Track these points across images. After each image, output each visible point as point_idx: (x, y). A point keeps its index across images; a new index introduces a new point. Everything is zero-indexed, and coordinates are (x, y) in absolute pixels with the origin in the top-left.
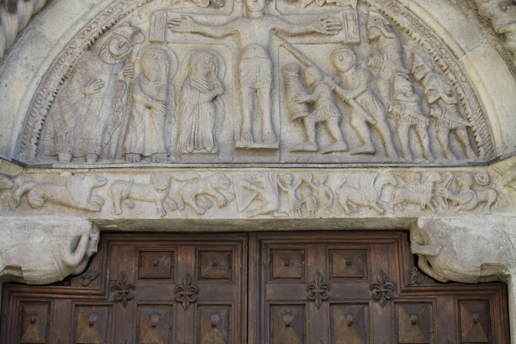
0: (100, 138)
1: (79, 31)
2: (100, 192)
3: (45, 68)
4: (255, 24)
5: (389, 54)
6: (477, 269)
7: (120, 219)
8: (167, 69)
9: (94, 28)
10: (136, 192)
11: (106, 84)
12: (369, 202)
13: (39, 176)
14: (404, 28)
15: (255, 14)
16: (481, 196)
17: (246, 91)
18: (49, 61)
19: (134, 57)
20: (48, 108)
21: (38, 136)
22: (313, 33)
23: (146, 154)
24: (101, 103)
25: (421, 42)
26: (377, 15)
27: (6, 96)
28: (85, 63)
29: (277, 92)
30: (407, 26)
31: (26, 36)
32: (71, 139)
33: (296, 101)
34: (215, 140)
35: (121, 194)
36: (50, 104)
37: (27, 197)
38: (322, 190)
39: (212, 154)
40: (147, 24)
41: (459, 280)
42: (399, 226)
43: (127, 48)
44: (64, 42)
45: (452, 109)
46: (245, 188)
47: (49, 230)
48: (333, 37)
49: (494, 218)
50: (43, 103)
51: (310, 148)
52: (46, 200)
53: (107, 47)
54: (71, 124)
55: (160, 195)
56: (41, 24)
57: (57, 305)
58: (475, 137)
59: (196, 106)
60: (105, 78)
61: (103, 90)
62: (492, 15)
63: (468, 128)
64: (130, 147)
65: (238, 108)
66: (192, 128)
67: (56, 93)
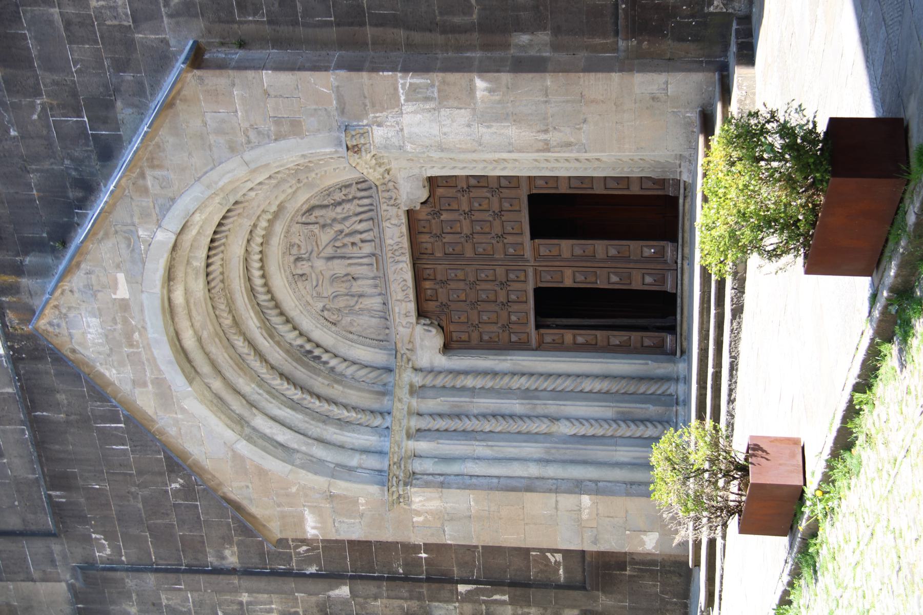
2: (404, 323)
3: (348, 342)
4: (315, 265)
10: (403, 312)
13: (399, 345)
15: (310, 264)
16: (392, 187)
18: (344, 340)
22: (316, 242)
26: (304, 217)
28: (343, 327)
34: (374, 278)
38: (395, 247)
44: (334, 335)
45: (348, 190)
47: (422, 340)
49: (401, 181)
52: (410, 342)
54: (372, 330)
55: (404, 304)
57: (452, 329)
59: (359, 286)
60: (349, 319)
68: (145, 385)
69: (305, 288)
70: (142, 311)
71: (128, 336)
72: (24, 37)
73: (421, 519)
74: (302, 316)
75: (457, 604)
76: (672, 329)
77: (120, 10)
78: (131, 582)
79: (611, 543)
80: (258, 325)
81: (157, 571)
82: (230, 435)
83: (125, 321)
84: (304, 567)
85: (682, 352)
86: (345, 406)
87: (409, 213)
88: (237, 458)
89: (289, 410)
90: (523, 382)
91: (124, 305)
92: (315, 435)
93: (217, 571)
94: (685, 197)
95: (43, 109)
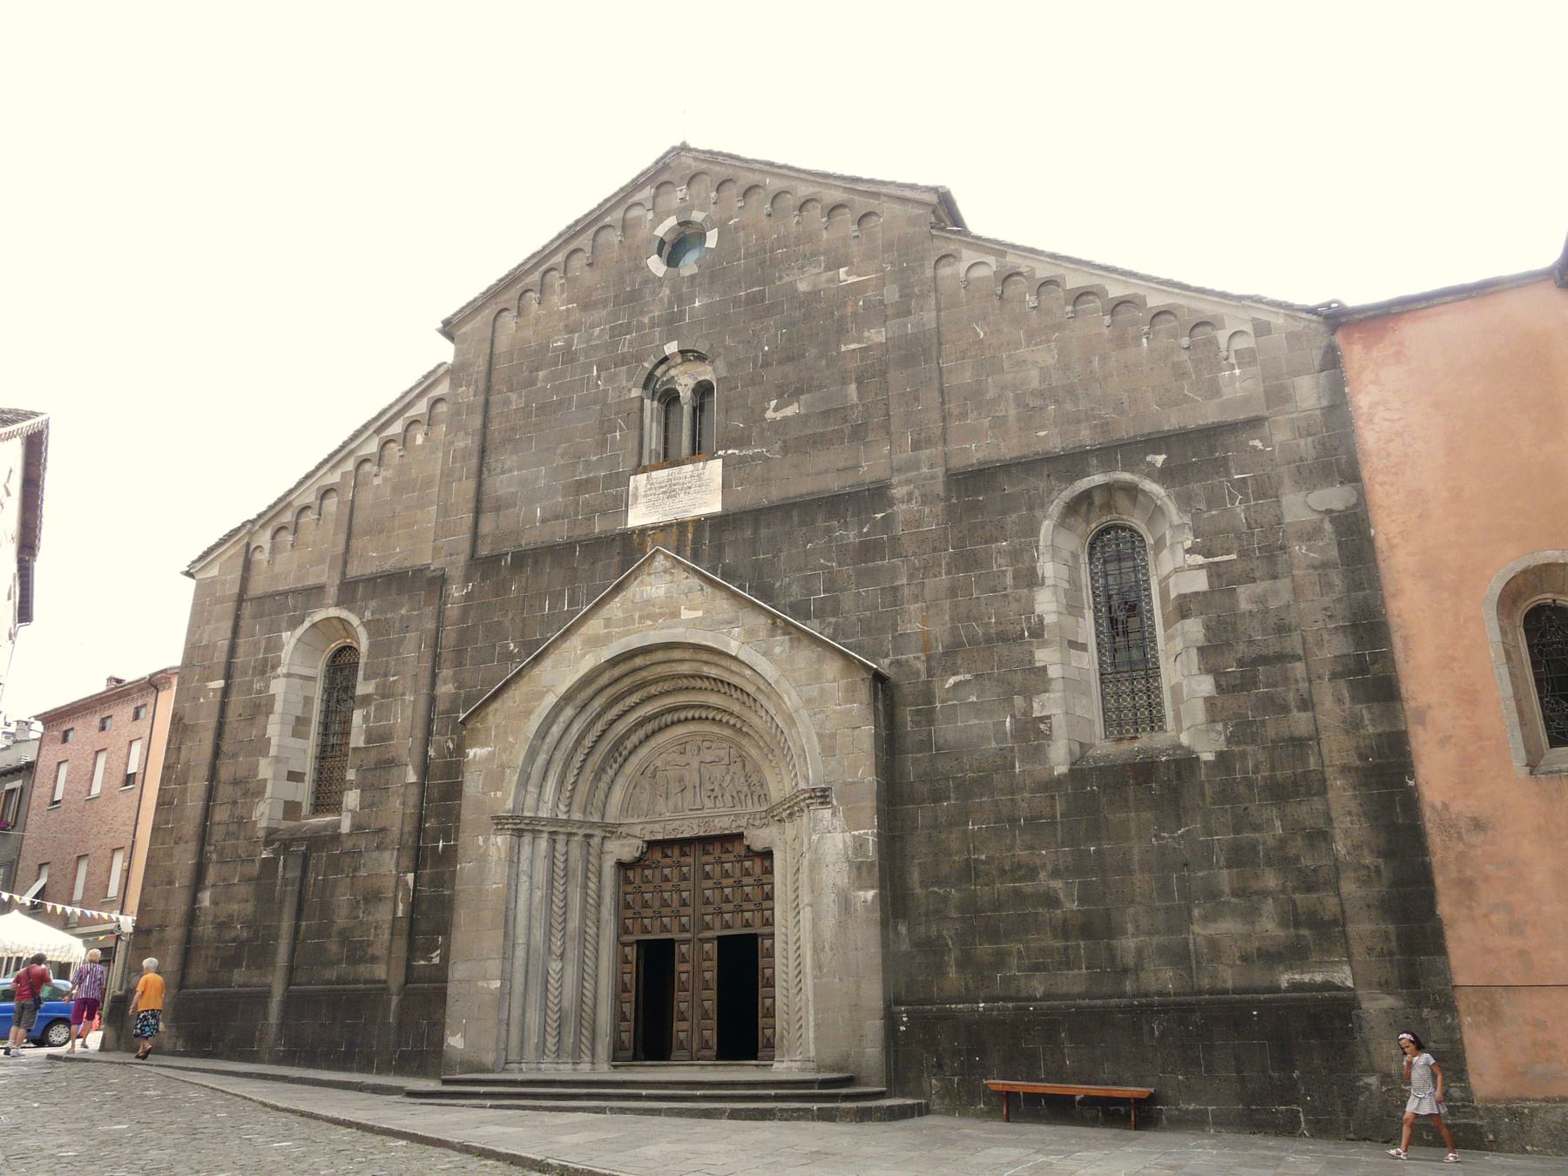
47: (630, 845)
68: (606, 627)
70: (670, 627)
71: (649, 617)
72: (883, 559)
73: (481, 843)
75: (394, 872)
76: (635, 1058)
77: (908, 625)
78: (430, 610)
79: (454, 1007)
81: (438, 629)
82: (562, 689)
83: (661, 615)
84: (434, 746)
85: (615, 1067)
86: (575, 782)
87: (740, 836)
88: (542, 695)
90: (592, 931)
91: (675, 614)
92: (555, 757)
93: (434, 676)
94: (757, 1066)
95: (827, 567)
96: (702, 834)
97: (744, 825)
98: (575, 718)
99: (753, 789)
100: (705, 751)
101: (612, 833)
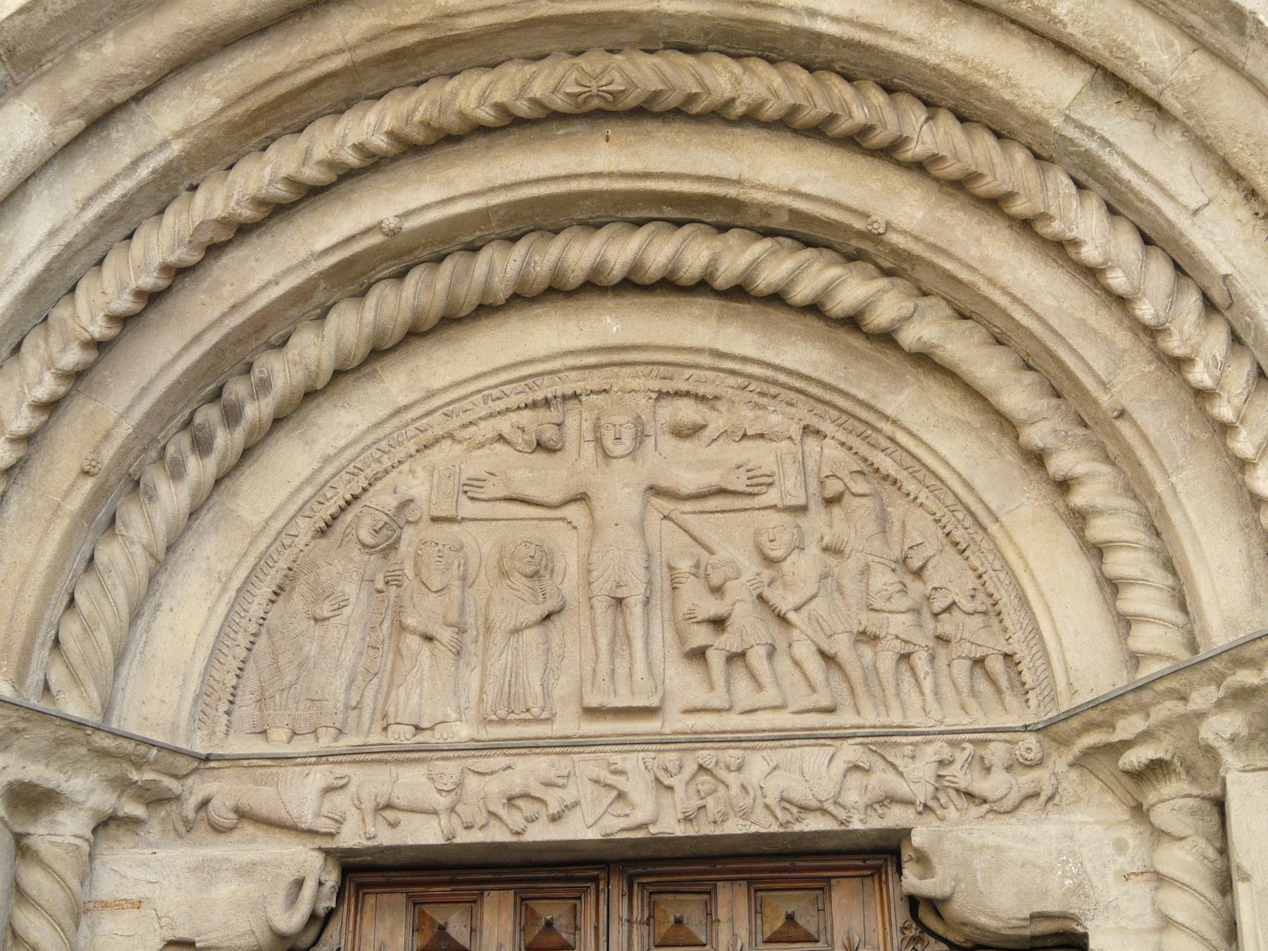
0: (342, 697)
1: (305, 504)
3: (242, 574)
5: (859, 525)
6: (1022, 923)
7: (375, 847)
8: (462, 568)
9: (331, 498)
11: (353, 600)
12: (821, 801)
14: (888, 476)
17: (601, 605)
18: (250, 561)
19: (403, 547)
20: (249, 645)
21: (231, 698)
22: (722, 492)
23: (424, 725)
24: (343, 634)
25: (919, 501)
27: (171, 629)
29: (659, 603)
30: (893, 473)
31: (207, 518)
32: (290, 701)
33: (690, 618)
35: (375, 800)
36: (252, 639)
37: (206, 812)
39: (542, 720)
40: (427, 486)
41: (994, 944)
42: (880, 843)
43: (390, 533)
44: (277, 525)
46: (596, 782)
47: (246, 871)
48: (759, 497)
50: (240, 637)
51: (716, 703)
52: (243, 815)
53: (354, 532)
56: (235, 495)
58: (1020, 673)
61: (347, 611)
62: (1042, 450)
63: (1007, 656)
64: (396, 712)
65: (589, 635)
66: (505, 675)
67: (264, 619)
69: (501, 438)
74: (382, 413)
80: (410, 224)
89: (35, 267)
96: (670, 826)
97: (922, 793)
98: (46, 165)
99: (947, 626)
100: (668, 443)
101: (156, 799)
